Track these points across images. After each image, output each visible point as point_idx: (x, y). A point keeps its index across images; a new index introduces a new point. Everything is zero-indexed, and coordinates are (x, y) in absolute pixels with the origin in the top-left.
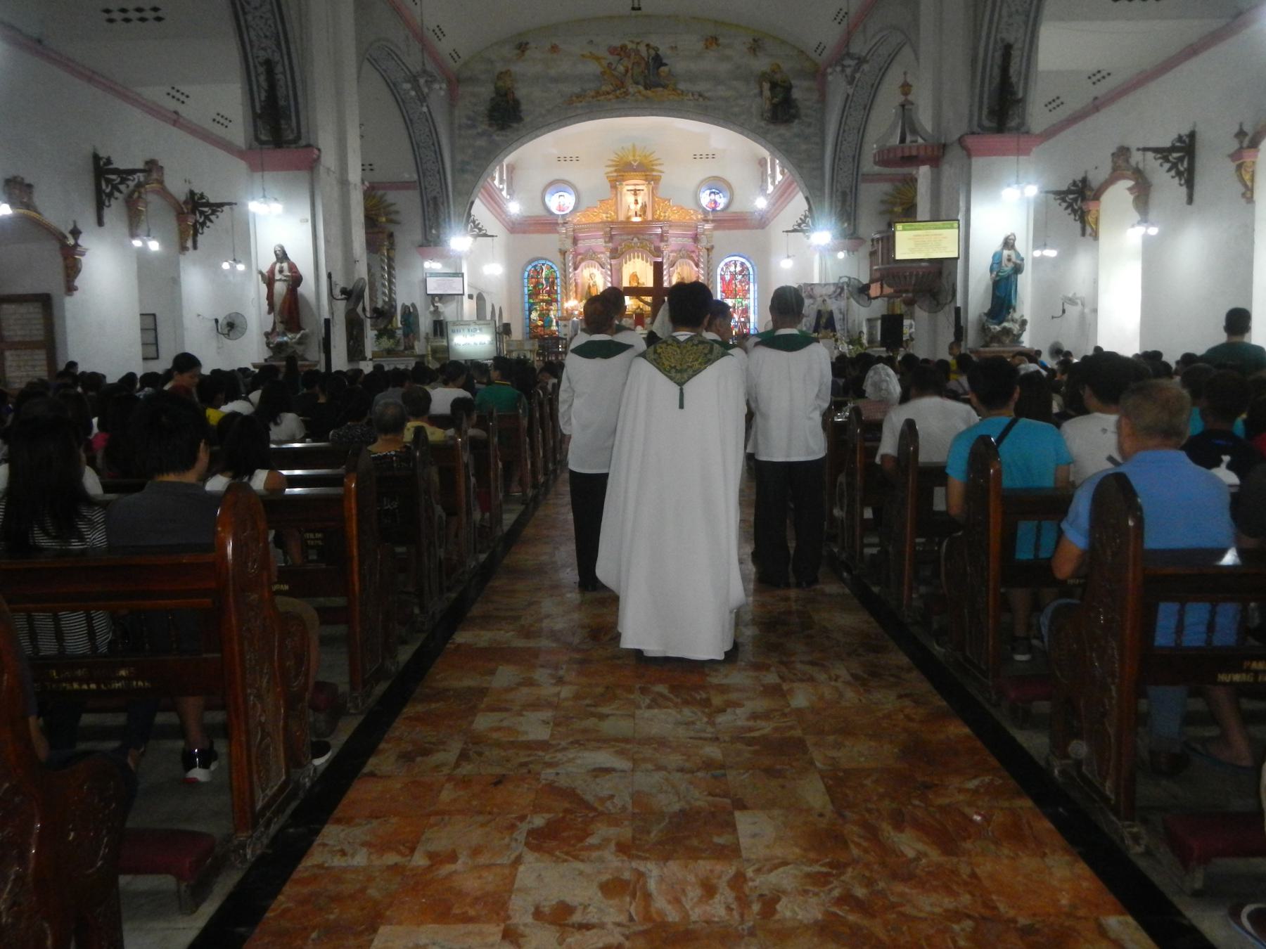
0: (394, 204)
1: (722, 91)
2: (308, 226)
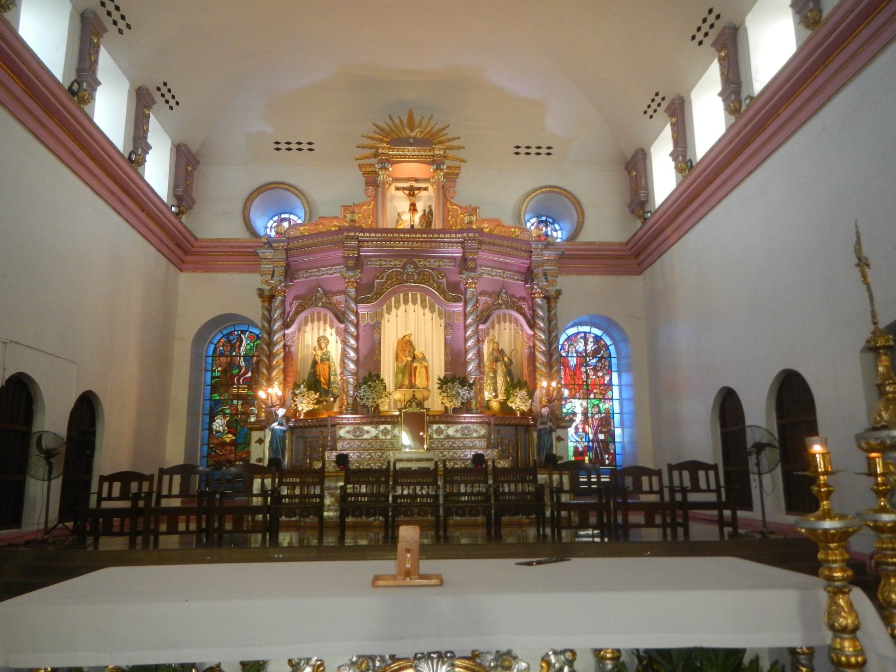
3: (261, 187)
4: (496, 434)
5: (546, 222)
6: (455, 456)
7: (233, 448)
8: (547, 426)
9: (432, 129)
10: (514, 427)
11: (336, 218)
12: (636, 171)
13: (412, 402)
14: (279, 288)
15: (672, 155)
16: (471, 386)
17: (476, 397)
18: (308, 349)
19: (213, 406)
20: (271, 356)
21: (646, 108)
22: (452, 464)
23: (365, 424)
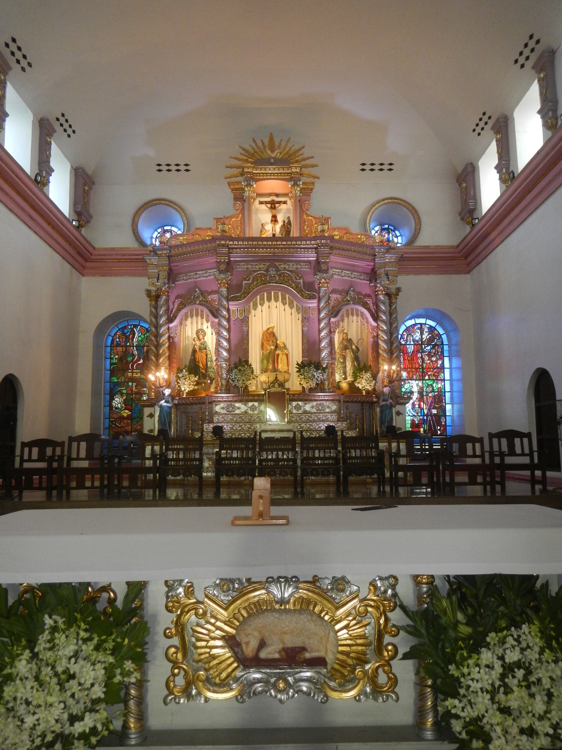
3: (146, 204)
4: (345, 410)
5: (388, 229)
6: (311, 427)
7: (129, 421)
8: (388, 403)
9: (289, 150)
10: (359, 404)
11: (210, 229)
12: (466, 183)
13: (275, 384)
14: (163, 289)
15: (496, 168)
16: (324, 369)
17: (328, 379)
18: (188, 340)
19: (112, 387)
20: (158, 346)
21: (474, 127)
22: (308, 434)
23: (236, 401)
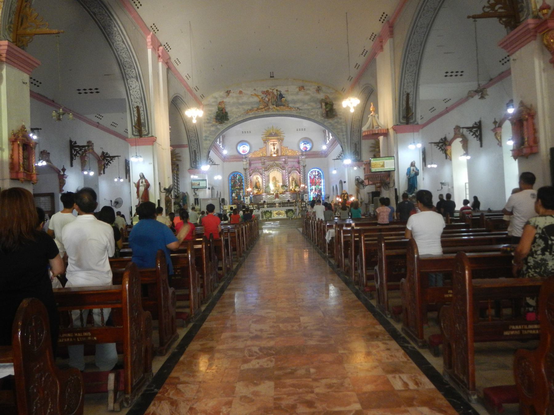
0: (179, 153)
1: (306, 106)
2: (152, 166)
5: (306, 144)
16: (287, 187)
